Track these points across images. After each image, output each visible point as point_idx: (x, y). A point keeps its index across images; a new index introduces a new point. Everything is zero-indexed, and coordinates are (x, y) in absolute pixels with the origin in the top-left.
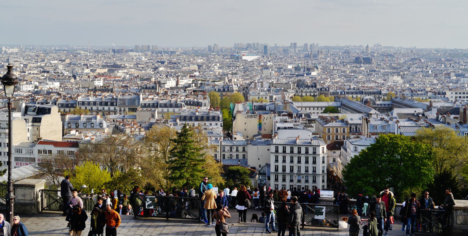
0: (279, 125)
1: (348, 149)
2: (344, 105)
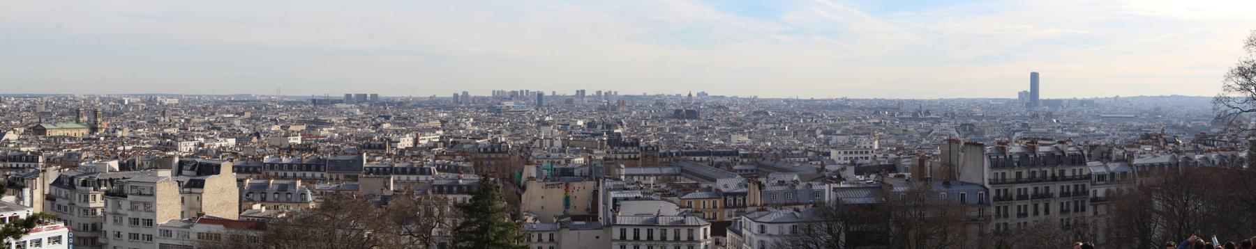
0: (613, 194)
1: (744, 231)
2: (687, 172)
